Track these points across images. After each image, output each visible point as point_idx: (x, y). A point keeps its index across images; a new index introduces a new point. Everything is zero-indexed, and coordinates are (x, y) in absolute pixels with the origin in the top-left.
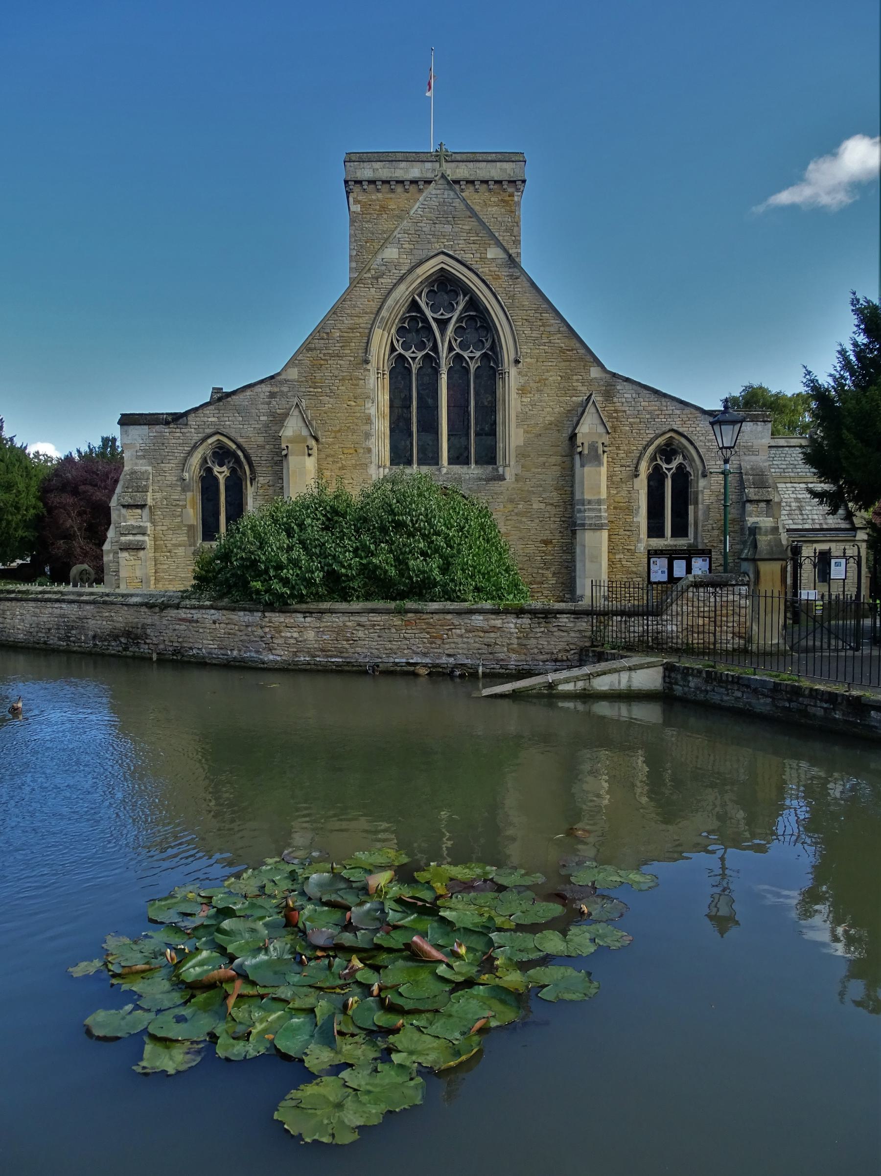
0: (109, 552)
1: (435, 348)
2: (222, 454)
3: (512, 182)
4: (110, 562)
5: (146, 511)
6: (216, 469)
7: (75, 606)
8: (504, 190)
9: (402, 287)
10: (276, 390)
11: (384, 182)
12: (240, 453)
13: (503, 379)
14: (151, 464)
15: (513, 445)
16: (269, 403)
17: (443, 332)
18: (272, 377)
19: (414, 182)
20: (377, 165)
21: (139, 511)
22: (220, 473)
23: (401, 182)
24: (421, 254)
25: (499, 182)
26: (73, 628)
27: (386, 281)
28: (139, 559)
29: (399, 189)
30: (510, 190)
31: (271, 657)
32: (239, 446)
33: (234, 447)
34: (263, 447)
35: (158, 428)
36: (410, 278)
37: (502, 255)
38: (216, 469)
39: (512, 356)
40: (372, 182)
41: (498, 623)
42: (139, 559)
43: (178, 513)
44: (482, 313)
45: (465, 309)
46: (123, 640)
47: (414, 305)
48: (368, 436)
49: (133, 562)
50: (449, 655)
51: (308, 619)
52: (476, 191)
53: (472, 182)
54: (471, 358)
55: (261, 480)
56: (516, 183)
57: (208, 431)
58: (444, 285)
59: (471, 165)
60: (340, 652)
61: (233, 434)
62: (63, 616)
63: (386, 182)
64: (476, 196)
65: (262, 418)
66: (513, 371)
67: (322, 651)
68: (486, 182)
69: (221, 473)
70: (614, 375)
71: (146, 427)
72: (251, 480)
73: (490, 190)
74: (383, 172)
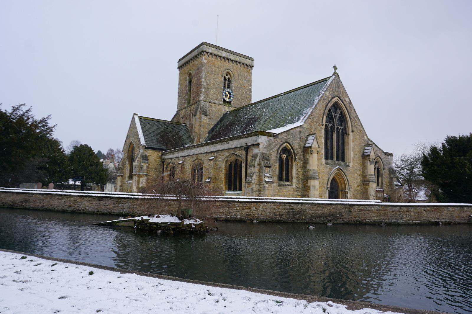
1: (334, 124)
2: (285, 150)
3: (250, 66)
4: (254, 188)
5: (271, 168)
6: (283, 155)
7: (299, 206)
9: (329, 104)
10: (301, 130)
12: (292, 150)
13: (348, 137)
14: (268, 151)
15: (351, 157)
16: (300, 134)
17: (336, 120)
18: (301, 126)
19: (224, 58)
20: (213, 49)
21: (269, 168)
22: (284, 156)
23: (220, 57)
24: (333, 95)
25: (247, 65)
26: (298, 214)
28: (271, 187)
29: (219, 59)
30: (250, 68)
31: (402, 221)
32: (292, 148)
33: (290, 148)
34: (297, 149)
35: (270, 138)
36: (331, 102)
37: (349, 101)
39: (351, 130)
40: (211, 54)
41: (453, 209)
42: (271, 187)
43: (275, 170)
44: (343, 116)
45: (340, 114)
46: (328, 218)
47: (330, 110)
48: (322, 149)
49: (269, 188)
50: (444, 219)
51: (412, 209)
52: (237, 65)
53: (240, 63)
54: (341, 129)
55: (297, 160)
56: (252, 67)
57: (284, 141)
58: (336, 106)
59: (240, 57)
60: (419, 219)
61: (291, 144)
62: (292, 209)
63: (216, 55)
64: (240, 67)
66: (351, 134)
67: (415, 219)
69: (284, 156)
70: (369, 139)
71: (267, 137)
72: (295, 160)
74: (215, 51)
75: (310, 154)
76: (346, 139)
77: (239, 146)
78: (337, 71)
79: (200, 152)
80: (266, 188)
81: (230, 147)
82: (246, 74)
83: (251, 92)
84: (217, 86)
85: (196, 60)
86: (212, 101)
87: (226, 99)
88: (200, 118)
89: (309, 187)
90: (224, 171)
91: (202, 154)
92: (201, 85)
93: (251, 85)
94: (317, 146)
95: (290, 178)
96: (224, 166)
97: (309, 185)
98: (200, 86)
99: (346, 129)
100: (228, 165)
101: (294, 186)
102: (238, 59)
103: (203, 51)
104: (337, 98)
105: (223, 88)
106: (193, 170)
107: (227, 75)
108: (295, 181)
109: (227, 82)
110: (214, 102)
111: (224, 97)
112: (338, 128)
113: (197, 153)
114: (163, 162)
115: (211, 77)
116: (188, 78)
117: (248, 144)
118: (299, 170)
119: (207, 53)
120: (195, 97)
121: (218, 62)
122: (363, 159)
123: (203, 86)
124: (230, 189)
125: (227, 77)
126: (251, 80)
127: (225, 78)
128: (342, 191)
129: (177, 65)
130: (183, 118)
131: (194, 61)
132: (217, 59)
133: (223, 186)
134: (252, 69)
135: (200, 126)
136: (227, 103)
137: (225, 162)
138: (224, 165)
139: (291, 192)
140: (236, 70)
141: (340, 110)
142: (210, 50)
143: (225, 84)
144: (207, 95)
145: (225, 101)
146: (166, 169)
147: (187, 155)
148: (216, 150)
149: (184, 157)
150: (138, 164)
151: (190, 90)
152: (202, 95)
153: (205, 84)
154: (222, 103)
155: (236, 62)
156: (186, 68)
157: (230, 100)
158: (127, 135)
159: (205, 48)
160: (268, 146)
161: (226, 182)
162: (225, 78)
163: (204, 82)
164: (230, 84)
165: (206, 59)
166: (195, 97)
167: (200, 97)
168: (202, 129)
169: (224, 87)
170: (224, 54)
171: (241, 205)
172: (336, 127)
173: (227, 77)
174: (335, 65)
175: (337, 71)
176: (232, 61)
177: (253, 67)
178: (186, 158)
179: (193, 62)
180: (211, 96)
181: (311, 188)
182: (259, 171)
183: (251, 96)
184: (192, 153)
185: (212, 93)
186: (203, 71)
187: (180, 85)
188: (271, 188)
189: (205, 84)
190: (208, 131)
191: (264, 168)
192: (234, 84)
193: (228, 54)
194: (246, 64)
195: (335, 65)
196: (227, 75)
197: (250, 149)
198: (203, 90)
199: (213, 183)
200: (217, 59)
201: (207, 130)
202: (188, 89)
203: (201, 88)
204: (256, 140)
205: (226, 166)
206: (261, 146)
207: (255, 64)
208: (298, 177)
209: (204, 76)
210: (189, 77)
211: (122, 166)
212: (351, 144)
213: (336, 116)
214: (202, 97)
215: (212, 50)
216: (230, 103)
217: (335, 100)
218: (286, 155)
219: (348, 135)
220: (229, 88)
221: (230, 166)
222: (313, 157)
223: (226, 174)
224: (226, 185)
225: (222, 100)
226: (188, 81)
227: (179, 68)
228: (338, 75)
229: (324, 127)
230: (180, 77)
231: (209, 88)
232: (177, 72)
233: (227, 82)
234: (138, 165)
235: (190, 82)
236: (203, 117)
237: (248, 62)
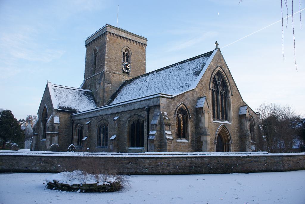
0: (155, 140)
2: (181, 110)
3: (145, 45)
6: (180, 115)
7: (200, 159)
8: (142, 46)
11: (116, 35)
12: (187, 111)
13: (229, 100)
18: (194, 89)
23: (120, 36)
27: (212, 70)
30: (144, 46)
33: (186, 108)
36: (215, 71)
38: (180, 115)
39: (231, 94)
40: (113, 34)
43: (173, 128)
47: (214, 78)
49: (170, 145)
51: (291, 158)
52: (133, 43)
56: (145, 45)
58: (219, 74)
64: (136, 45)
65: (191, 101)
66: (231, 97)
68: (139, 43)
69: (181, 115)
70: (244, 101)
73: (139, 45)
74: (116, 32)
75: (202, 114)
76: (227, 101)
77: (141, 107)
78: (218, 46)
79: (105, 113)
80: (167, 144)
81: (133, 108)
82: (141, 51)
83: (145, 65)
84: (118, 60)
85: (100, 38)
86: (114, 72)
87: (125, 70)
88: (104, 85)
89: (202, 142)
90: (127, 130)
91: (107, 115)
92: (105, 58)
93: (145, 60)
94: (208, 107)
95: (186, 135)
96: (127, 126)
97: (202, 140)
98: (104, 59)
99: (227, 93)
100: (130, 125)
101: (190, 142)
102: (134, 38)
103: (107, 32)
104: (219, 68)
105: (122, 61)
106: (99, 130)
107: (126, 51)
108: (190, 137)
109: (126, 57)
110: (115, 72)
111: (124, 68)
112: (221, 92)
113: (103, 114)
114: (73, 123)
115: (113, 52)
116: (93, 53)
117: (150, 105)
118: (193, 128)
119: (110, 33)
120: (100, 68)
121: (119, 40)
122: (240, 117)
123: (106, 59)
124: (133, 146)
125: (126, 53)
126: (145, 56)
127: (124, 53)
128: (225, 144)
129: (84, 44)
130: (89, 86)
131: (98, 40)
132: (117, 38)
133: (126, 142)
134: (146, 47)
135: (104, 91)
136: (125, 74)
137: (128, 121)
138: (127, 124)
139: (187, 147)
140: (133, 47)
141: (222, 77)
142: (112, 31)
143: (124, 58)
144: (110, 67)
145: (124, 72)
146: (75, 129)
147: (93, 116)
148: (120, 111)
149: (91, 118)
150: (51, 125)
151: (95, 63)
152: (105, 66)
153: (108, 58)
154: (122, 73)
155: (133, 41)
156: (92, 46)
157: (128, 71)
158: (42, 100)
159: (108, 29)
160: (167, 107)
161: (129, 139)
162: (124, 53)
163: (107, 56)
164: (128, 58)
165: (108, 38)
166: (100, 68)
167: (104, 68)
168: (106, 95)
169: (124, 60)
170: (123, 35)
171: (148, 161)
172: (219, 91)
173: (126, 53)
174: (217, 41)
175: (218, 46)
176: (130, 40)
177: (147, 45)
178: (93, 119)
179: (98, 41)
180: (113, 68)
181: (204, 142)
182: (160, 129)
183: (145, 68)
184: (97, 115)
185: (113, 65)
186: (107, 47)
187: (86, 59)
188: (171, 144)
189: (108, 58)
190: (110, 96)
191: (165, 126)
192: (132, 58)
193: (127, 34)
194: (142, 44)
195: (217, 41)
196: (126, 51)
197: (151, 110)
198: (106, 62)
199: (118, 140)
200: (117, 38)
201: (110, 96)
202: (93, 62)
203: (104, 61)
204: (157, 102)
205: (129, 125)
206: (161, 107)
207: (148, 43)
208: (192, 133)
209: (107, 51)
210: (94, 52)
211: (37, 127)
212: (232, 106)
213: (219, 82)
214: (106, 68)
215: (114, 31)
216: (128, 73)
217: (218, 69)
218: (182, 115)
219: (229, 99)
220: (127, 61)
221: (133, 125)
222: (204, 117)
223: (129, 132)
224: (129, 142)
225: (122, 71)
226: (93, 56)
227: (86, 46)
228: (219, 49)
229: (211, 91)
230: (86, 53)
231: (111, 61)
232: (85, 49)
233: (126, 57)
234: (51, 126)
235: (95, 57)
236: (106, 85)
237: (142, 41)
